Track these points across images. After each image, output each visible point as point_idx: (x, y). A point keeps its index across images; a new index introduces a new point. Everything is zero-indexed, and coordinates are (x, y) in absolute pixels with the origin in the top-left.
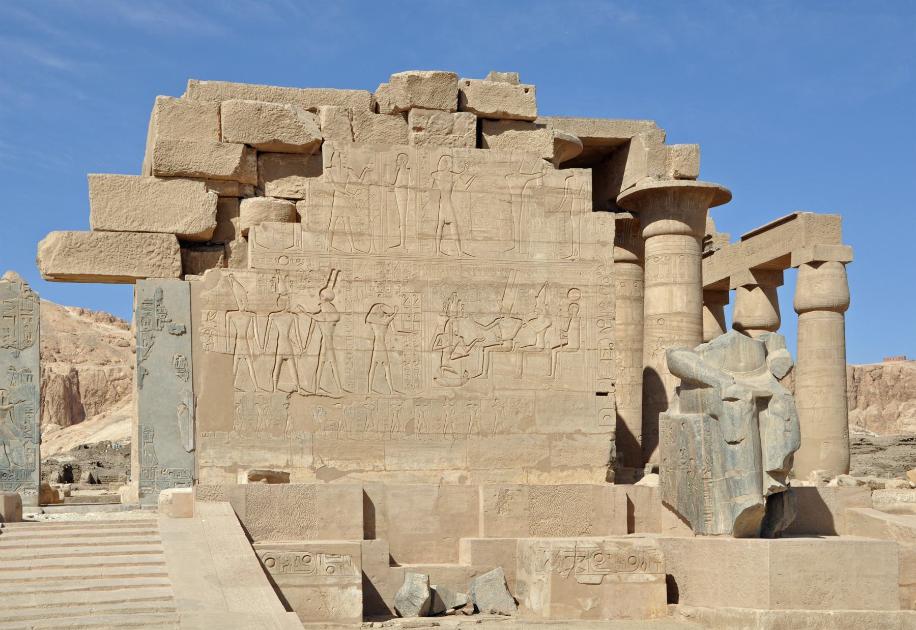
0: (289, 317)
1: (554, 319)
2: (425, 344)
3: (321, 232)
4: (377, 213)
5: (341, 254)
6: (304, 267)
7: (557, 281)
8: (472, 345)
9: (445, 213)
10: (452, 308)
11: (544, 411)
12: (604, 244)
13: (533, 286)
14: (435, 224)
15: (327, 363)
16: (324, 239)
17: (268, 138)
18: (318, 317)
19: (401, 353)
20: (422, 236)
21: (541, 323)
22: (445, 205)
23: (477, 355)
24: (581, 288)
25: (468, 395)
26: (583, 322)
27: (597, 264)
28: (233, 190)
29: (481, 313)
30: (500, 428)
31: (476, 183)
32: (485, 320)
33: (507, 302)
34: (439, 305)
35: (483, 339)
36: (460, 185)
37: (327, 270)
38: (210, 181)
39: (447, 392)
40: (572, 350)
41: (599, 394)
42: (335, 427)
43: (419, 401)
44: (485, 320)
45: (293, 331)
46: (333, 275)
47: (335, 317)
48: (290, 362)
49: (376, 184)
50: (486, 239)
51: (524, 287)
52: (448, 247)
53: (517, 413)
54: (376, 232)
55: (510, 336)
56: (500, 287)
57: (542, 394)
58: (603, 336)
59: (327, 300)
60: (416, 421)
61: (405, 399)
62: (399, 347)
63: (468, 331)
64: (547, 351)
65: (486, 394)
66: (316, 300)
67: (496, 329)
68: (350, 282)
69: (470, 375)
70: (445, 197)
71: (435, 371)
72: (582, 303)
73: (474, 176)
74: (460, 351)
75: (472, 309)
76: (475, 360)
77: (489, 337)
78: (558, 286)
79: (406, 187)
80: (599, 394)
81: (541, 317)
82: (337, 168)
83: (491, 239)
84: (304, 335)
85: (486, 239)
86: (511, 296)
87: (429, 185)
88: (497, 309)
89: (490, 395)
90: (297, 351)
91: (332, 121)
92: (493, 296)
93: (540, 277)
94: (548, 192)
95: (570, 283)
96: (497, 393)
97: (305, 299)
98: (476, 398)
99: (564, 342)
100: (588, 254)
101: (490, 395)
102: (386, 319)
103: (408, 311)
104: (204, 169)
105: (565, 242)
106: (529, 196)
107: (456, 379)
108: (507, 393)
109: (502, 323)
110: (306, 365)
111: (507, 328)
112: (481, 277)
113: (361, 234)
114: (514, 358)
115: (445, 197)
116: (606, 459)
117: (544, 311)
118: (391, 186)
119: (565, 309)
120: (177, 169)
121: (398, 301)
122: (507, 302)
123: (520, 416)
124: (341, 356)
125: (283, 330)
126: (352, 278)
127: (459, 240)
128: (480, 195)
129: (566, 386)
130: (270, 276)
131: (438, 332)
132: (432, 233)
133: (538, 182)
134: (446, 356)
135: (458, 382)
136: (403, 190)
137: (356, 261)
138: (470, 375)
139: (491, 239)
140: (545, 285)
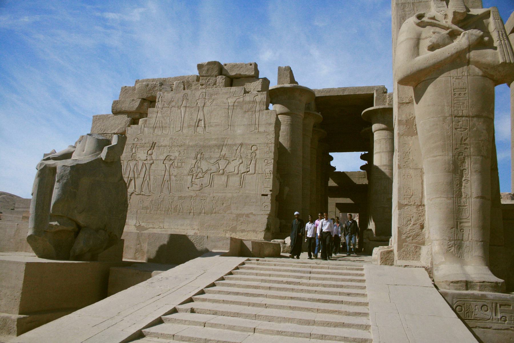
0: (135, 162)
1: (244, 160)
2: (186, 172)
3: (151, 127)
4: (173, 118)
5: (158, 135)
6: (143, 142)
7: (246, 142)
8: (206, 172)
9: (200, 116)
10: (199, 156)
11: (236, 203)
12: (270, 124)
13: (235, 145)
14: (195, 121)
15: (146, 182)
16: (152, 131)
17: (149, 95)
18: (146, 162)
19: (175, 176)
20: (189, 126)
21: (237, 162)
22: (201, 114)
23: (207, 176)
24: (258, 145)
25: (202, 195)
26: (258, 161)
27: (266, 134)
28: (137, 116)
29: (211, 158)
30: (214, 211)
31: (215, 102)
32: (212, 161)
33: (223, 153)
34: (193, 155)
35: (211, 169)
36: (208, 104)
37: (152, 143)
38: (128, 113)
39: (193, 194)
40: (251, 174)
41: (263, 195)
42: (147, 208)
43: (180, 198)
44: (212, 161)
45: (135, 168)
46: (153, 145)
47: (152, 162)
48: (133, 181)
49: (174, 107)
50: (216, 125)
51: (231, 146)
52: (200, 130)
53: (223, 204)
54: (172, 126)
55: (223, 168)
56: (220, 147)
57: (235, 195)
58: (267, 167)
59: (150, 155)
60: (178, 206)
61: (175, 197)
62: (175, 174)
63: (204, 165)
64: (239, 175)
65: (210, 195)
66: (146, 155)
67: (217, 165)
68: (159, 147)
69: (204, 186)
70: (201, 109)
71: (189, 184)
72: (257, 152)
73: (214, 100)
74: (200, 175)
75: (207, 156)
76: (206, 180)
77: (214, 168)
78: (247, 145)
79: (186, 107)
80: (263, 195)
81: (238, 159)
82: (160, 102)
83: (218, 125)
84: (140, 169)
85: (216, 125)
86: (225, 151)
87: (195, 105)
88: (218, 156)
89: (211, 195)
90: (136, 176)
91: (177, 86)
92: (217, 150)
93: (239, 142)
94: (245, 103)
95: (253, 143)
96: (215, 195)
97: (142, 155)
98: (205, 196)
99: (248, 170)
100: (262, 129)
101: (211, 195)
102: (171, 162)
103: (180, 158)
104: (127, 109)
105: (252, 124)
106: (237, 106)
107: (197, 187)
108: (220, 195)
109: (220, 162)
110: (139, 182)
111: (222, 164)
112: (213, 142)
113: (166, 127)
114: (224, 178)
115: (201, 109)
116: (264, 227)
117: (239, 156)
118: (179, 107)
119: (250, 155)
120: (118, 110)
121: (177, 154)
122: (223, 153)
123: (224, 205)
124: (152, 177)
125: (132, 167)
126: (160, 145)
127: (205, 127)
128: (216, 107)
129: (247, 191)
130: (130, 146)
131: (192, 167)
132: (194, 124)
133: (241, 99)
134: (194, 177)
135: (198, 189)
136: (184, 108)
137: (162, 138)
138: (204, 186)
139: (218, 125)
140: (241, 145)
